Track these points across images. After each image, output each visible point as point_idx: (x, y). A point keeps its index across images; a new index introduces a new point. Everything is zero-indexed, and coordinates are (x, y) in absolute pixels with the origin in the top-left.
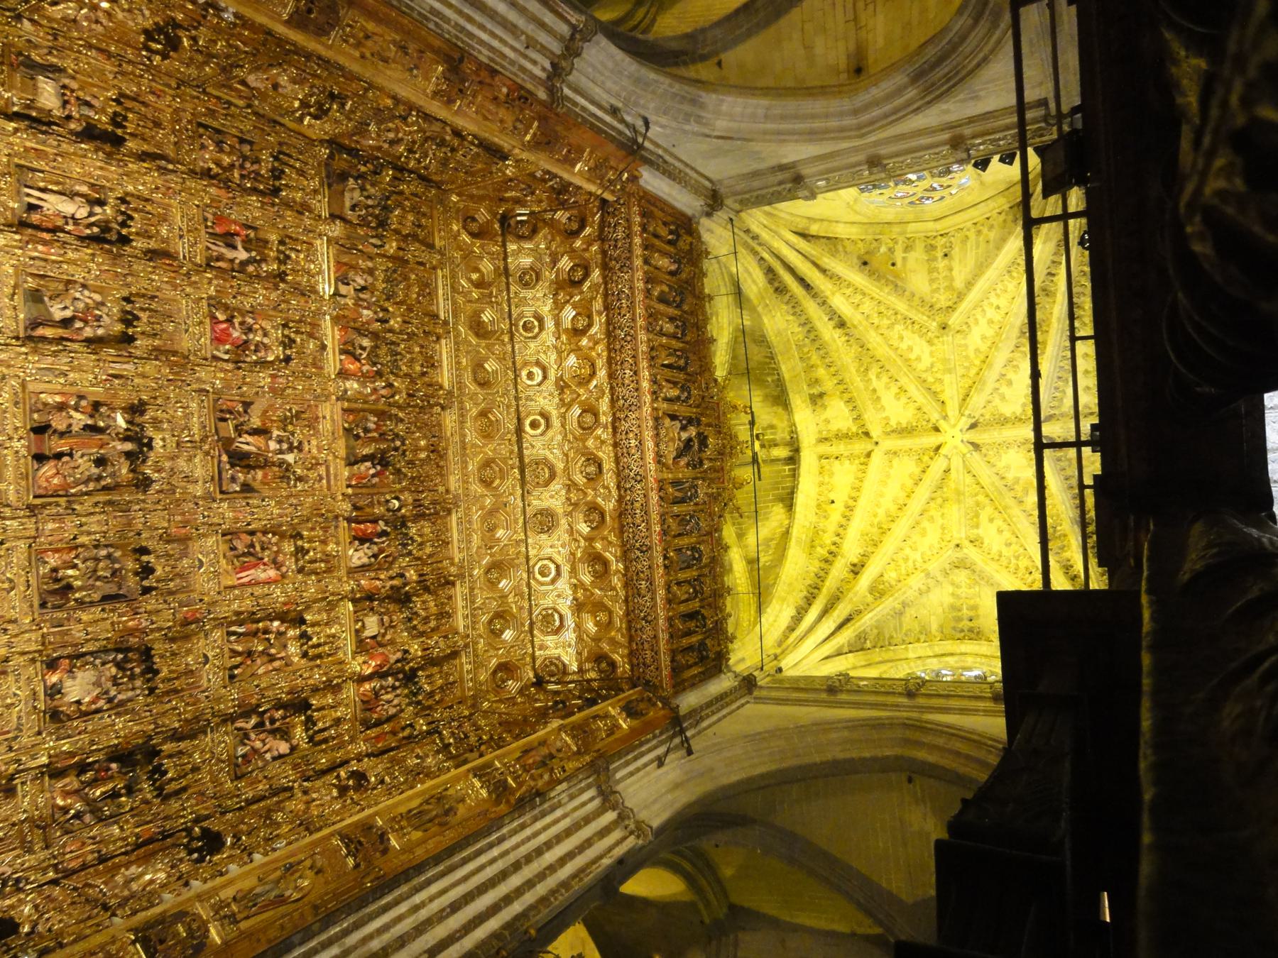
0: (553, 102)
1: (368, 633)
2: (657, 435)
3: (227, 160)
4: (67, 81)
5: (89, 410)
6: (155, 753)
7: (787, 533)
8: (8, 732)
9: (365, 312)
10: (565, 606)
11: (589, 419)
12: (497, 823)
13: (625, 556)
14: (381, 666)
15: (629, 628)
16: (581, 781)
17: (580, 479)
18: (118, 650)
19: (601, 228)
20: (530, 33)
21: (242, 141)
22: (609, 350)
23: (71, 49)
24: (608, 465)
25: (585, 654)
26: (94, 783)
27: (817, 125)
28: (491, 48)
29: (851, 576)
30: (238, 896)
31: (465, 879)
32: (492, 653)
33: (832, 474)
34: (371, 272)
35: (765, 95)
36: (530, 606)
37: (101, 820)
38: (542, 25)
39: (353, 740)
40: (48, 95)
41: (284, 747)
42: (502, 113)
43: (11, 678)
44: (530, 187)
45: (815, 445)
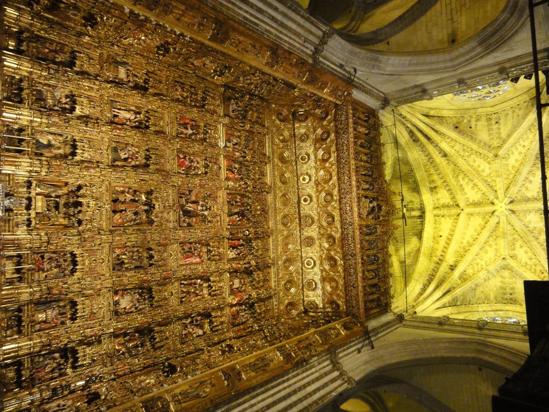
0: (315, 64)
1: (235, 286)
2: (359, 205)
3: (185, 94)
4: (129, 68)
5: (132, 193)
6: (151, 331)
7: (419, 250)
8: (99, 318)
9: (237, 153)
10: (317, 278)
11: (329, 198)
12: (287, 372)
13: (344, 258)
14: (240, 301)
15: (346, 290)
16: (323, 357)
17: (325, 224)
18: (140, 288)
19: (335, 116)
20: (306, 36)
21: (191, 87)
22: (338, 169)
23: (131, 55)
24: (337, 218)
25: (326, 300)
26: (129, 341)
27: (433, 67)
28: (290, 44)
29: (450, 271)
30: (182, 392)
31: (273, 395)
32: (286, 298)
33: (440, 224)
34: (239, 137)
35: (409, 55)
36: (303, 278)
37: (131, 356)
38: (311, 32)
39: (228, 331)
40: (122, 73)
41: (201, 332)
42: (293, 70)
43: (101, 297)
44: (305, 100)
45: (432, 210)
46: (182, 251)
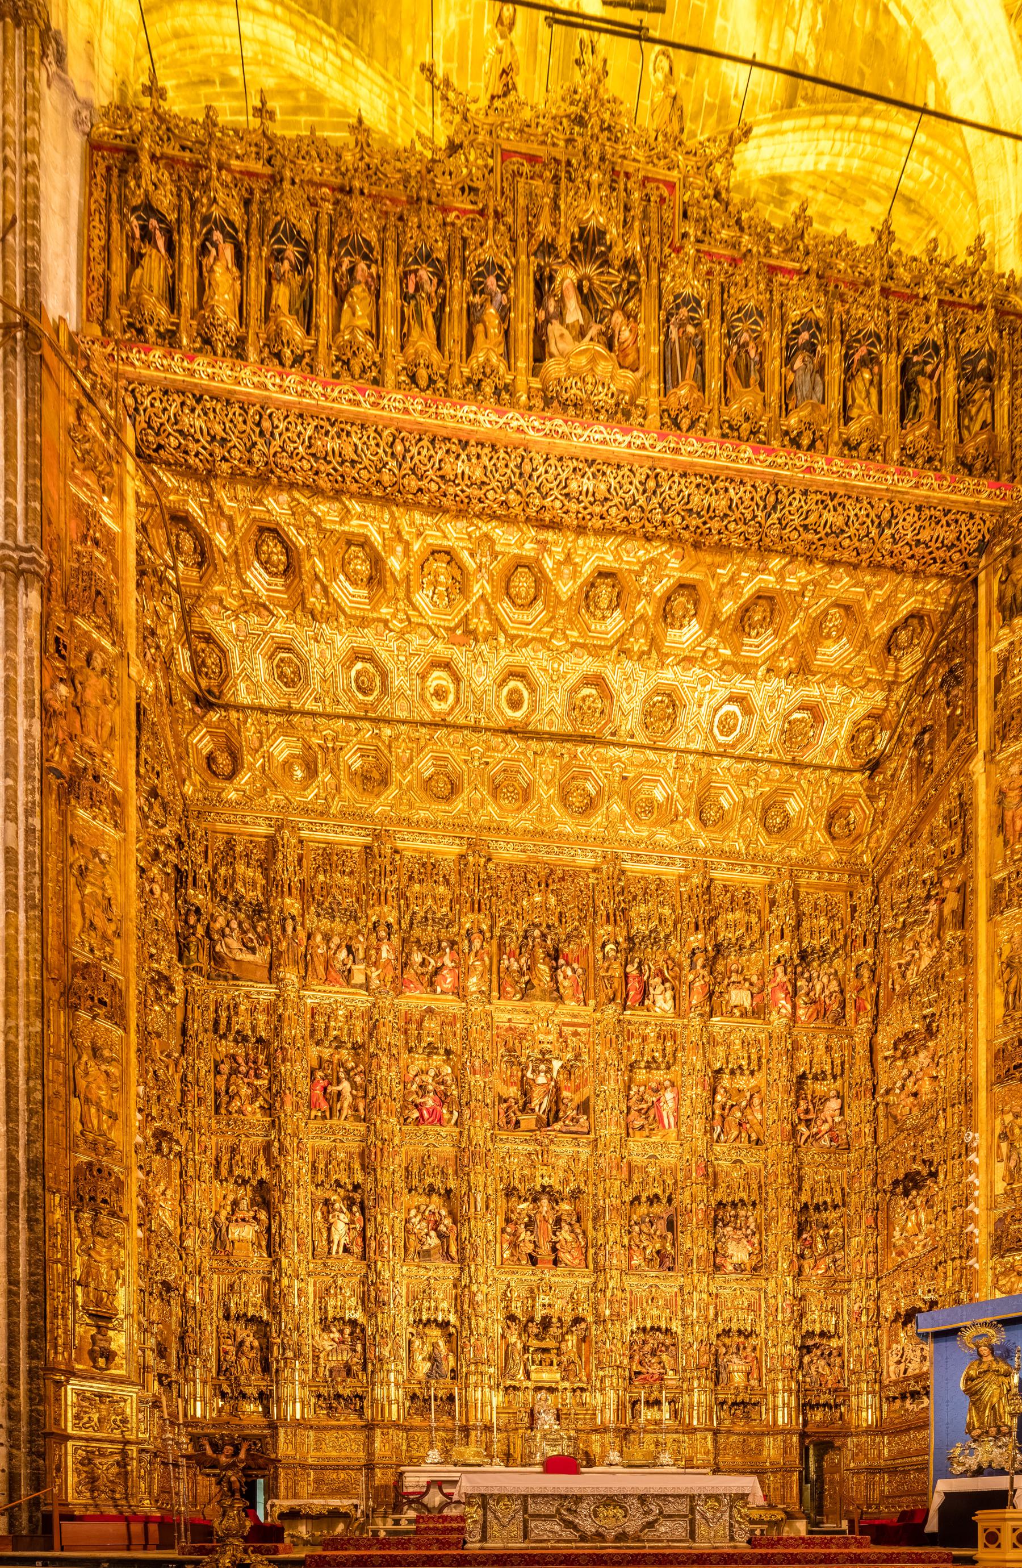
46: (646, 1132)
